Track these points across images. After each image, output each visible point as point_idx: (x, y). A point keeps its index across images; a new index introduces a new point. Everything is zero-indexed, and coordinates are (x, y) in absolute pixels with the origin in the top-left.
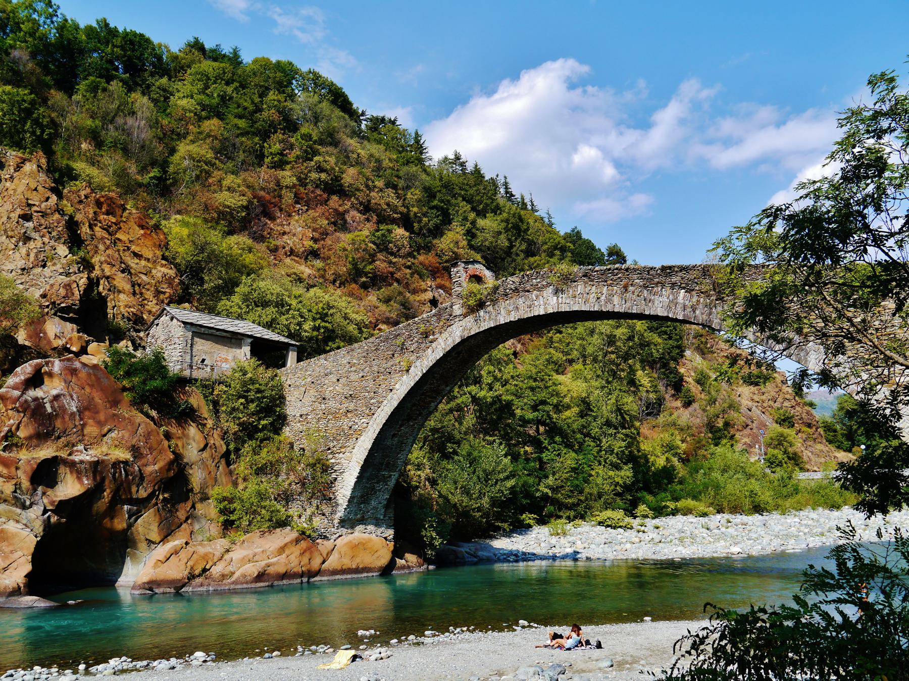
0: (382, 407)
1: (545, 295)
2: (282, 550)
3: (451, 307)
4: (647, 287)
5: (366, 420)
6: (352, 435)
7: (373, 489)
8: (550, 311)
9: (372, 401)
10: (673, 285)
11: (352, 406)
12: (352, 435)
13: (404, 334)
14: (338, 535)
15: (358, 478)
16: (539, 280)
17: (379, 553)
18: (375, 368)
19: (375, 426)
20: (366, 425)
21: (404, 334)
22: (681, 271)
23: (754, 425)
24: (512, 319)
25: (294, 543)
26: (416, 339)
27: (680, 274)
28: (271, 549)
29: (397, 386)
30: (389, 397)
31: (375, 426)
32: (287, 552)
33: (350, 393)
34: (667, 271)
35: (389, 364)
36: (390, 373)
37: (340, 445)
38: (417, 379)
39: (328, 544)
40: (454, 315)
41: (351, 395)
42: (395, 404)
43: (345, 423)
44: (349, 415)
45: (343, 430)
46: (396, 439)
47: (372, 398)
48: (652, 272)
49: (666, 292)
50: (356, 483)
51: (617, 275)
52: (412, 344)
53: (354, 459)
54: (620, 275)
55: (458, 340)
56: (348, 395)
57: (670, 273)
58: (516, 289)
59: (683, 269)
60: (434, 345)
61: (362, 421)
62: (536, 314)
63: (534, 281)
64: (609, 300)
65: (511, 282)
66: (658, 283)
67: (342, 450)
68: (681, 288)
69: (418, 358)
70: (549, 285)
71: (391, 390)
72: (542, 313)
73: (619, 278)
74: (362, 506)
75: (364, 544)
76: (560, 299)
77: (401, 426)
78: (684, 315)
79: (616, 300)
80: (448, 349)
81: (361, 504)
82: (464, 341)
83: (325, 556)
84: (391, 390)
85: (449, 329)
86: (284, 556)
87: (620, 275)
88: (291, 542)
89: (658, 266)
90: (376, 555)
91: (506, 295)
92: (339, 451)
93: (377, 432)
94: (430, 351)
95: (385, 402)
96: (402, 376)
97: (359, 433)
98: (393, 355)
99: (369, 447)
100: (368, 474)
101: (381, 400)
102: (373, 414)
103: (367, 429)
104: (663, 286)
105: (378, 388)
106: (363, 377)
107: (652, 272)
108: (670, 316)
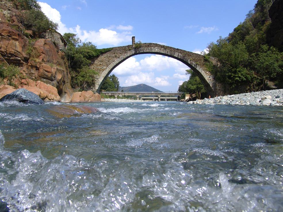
0: (111, 65)
9: (108, 63)
11: (101, 63)
29: (116, 60)
30: (113, 63)
31: (109, 69)
34: (178, 49)
43: (100, 67)
44: (101, 65)
49: (178, 53)
59: (181, 50)
62: (153, 51)
64: (168, 52)
69: (122, 55)
72: (154, 51)
89: (176, 48)
94: (125, 54)
96: (117, 58)
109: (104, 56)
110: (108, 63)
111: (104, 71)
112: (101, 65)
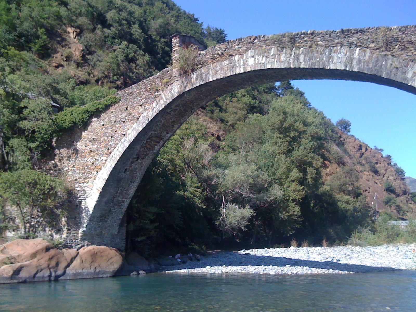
0: (117, 148)
1: (244, 58)
2: (34, 255)
3: (171, 70)
4: (329, 47)
5: (105, 158)
6: (94, 169)
7: (110, 211)
8: (249, 69)
9: (110, 143)
10: (350, 45)
11: (94, 148)
12: (94, 169)
13: (135, 92)
14: (80, 245)
15: (97, 201)
16: (240, 46)
17: (113, 260)
18: (113, 119)
19: (111, 161)
20: (104, 161)
21: (135, 92)
22: (357, 33)
23: (370, 190)
24: (219, 77)
25: (45, 250)
26: (144, 96)
27: (356, 35)
28: (25, 254)
29: (129, 132)
30: (123, 140)
32: (38, 257)
33: (93, 137)
34: (345, 33)
35: (124, 115)
36: (124, 122)
37: (84, 177)
38: (144, 125)
39: (73, 251)
40: (174, 76)
41: (94, 139)
42: (127, 145)
44: (92, 154)
45: (87, 166)
46: (128, 173)
47: (109, 141)
48: (332, 35)
49: (344, 50)
50: (96, 205)
51: (303, 38)
52: (141, 100)
53: (95, 188)
54: (306, 39)
55: (176, 95)
56: (92, 139)
57: (348, 34)
58: (222, 54)
60: (158, 99)
61: (102, 158)
62: (237, 72)
63: (236, 47)
65: (218, 49)
66: (338, 43)
67: (86, 181)
68: (357, 46)
69: (145, 110)
70: (248, 49)
71: (124, 135)
72: (242, 71)
73: (305, 41)
74: (101, 223)
75: (101, 253)
76: (257, 60)
77: (132, 163)
78: (359, 68)
79: (302, 58)
80: (168, 102)
81: (101, 221)
82: (181, 96)
83: (69, 260)
84: (124, 135)
85: (170, 87)
86: (36, 260)
87: (306, 39)
88: (42, 250)
90: (110, 261)
91: (214, 59)
92: (83, 181)
93: (113, 166)
94: (154, 104)
95: (120, 144)
97: (100, 167)
98: (127, 109)
99: (107, 178)
100: (105, 199)
101: (117, 142)
102: (110, 153)
103: (105, 165)
104: (342, 45)
105: (115, 134)
106: (103, 125)
107: (332, 35)
108: (347, 69)
109: (102, 124)
110: (110, 143)
111: (100, 169)
112: (94, 151)
